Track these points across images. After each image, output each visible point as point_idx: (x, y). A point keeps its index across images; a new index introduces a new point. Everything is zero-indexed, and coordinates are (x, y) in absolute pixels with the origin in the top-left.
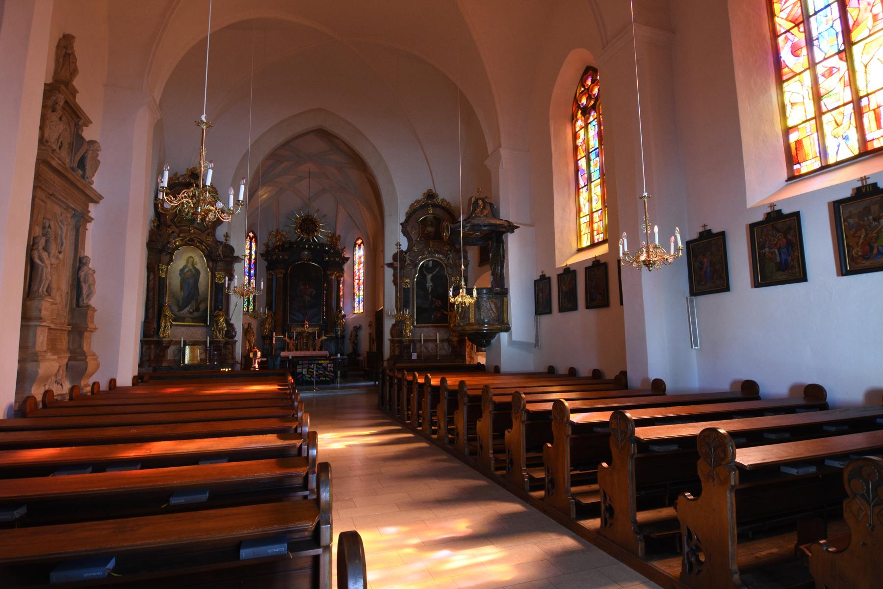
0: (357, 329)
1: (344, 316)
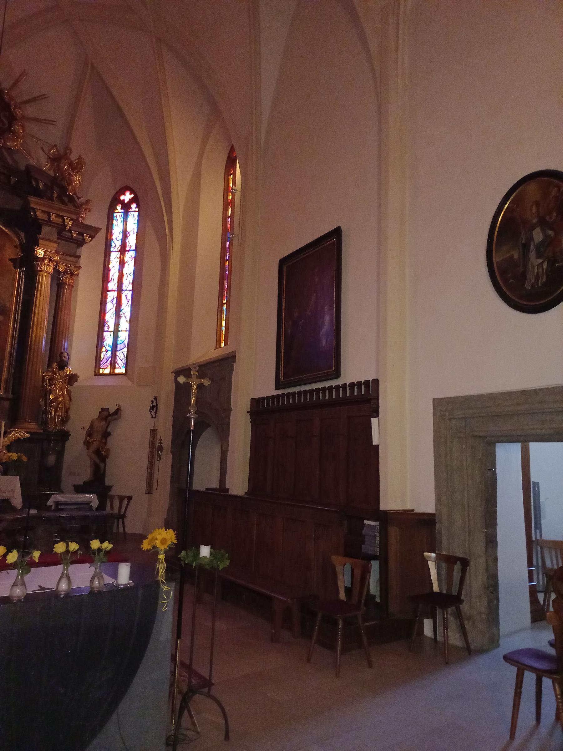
0: (109, 417)
1: (72, 379)
